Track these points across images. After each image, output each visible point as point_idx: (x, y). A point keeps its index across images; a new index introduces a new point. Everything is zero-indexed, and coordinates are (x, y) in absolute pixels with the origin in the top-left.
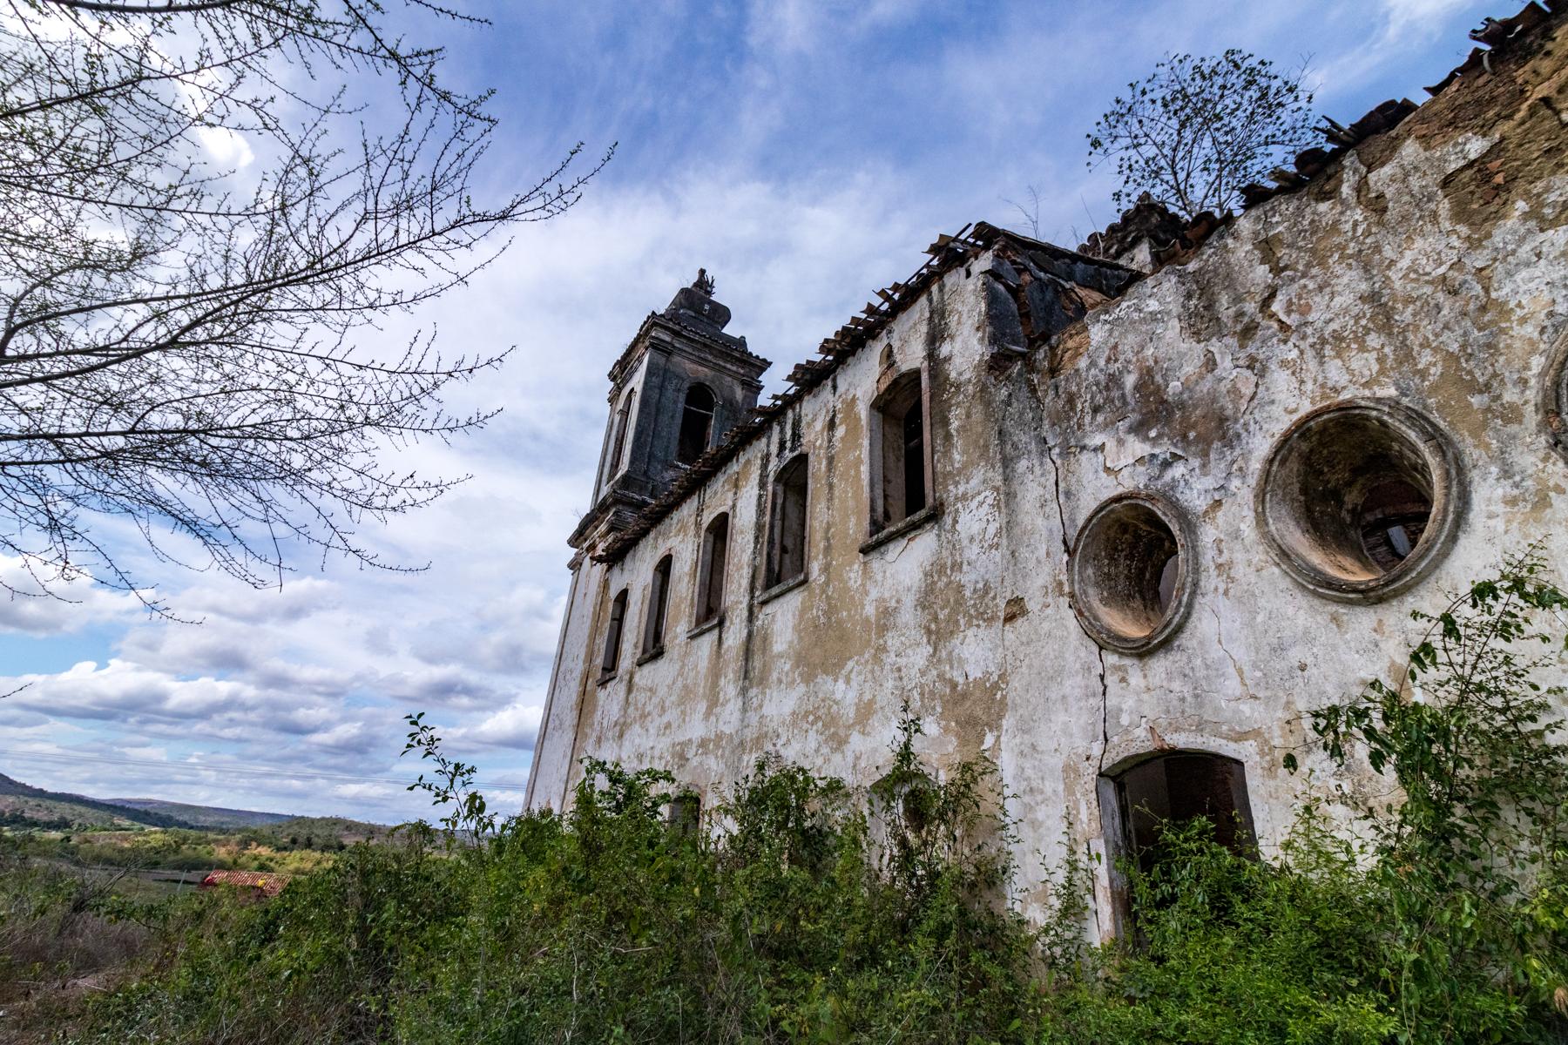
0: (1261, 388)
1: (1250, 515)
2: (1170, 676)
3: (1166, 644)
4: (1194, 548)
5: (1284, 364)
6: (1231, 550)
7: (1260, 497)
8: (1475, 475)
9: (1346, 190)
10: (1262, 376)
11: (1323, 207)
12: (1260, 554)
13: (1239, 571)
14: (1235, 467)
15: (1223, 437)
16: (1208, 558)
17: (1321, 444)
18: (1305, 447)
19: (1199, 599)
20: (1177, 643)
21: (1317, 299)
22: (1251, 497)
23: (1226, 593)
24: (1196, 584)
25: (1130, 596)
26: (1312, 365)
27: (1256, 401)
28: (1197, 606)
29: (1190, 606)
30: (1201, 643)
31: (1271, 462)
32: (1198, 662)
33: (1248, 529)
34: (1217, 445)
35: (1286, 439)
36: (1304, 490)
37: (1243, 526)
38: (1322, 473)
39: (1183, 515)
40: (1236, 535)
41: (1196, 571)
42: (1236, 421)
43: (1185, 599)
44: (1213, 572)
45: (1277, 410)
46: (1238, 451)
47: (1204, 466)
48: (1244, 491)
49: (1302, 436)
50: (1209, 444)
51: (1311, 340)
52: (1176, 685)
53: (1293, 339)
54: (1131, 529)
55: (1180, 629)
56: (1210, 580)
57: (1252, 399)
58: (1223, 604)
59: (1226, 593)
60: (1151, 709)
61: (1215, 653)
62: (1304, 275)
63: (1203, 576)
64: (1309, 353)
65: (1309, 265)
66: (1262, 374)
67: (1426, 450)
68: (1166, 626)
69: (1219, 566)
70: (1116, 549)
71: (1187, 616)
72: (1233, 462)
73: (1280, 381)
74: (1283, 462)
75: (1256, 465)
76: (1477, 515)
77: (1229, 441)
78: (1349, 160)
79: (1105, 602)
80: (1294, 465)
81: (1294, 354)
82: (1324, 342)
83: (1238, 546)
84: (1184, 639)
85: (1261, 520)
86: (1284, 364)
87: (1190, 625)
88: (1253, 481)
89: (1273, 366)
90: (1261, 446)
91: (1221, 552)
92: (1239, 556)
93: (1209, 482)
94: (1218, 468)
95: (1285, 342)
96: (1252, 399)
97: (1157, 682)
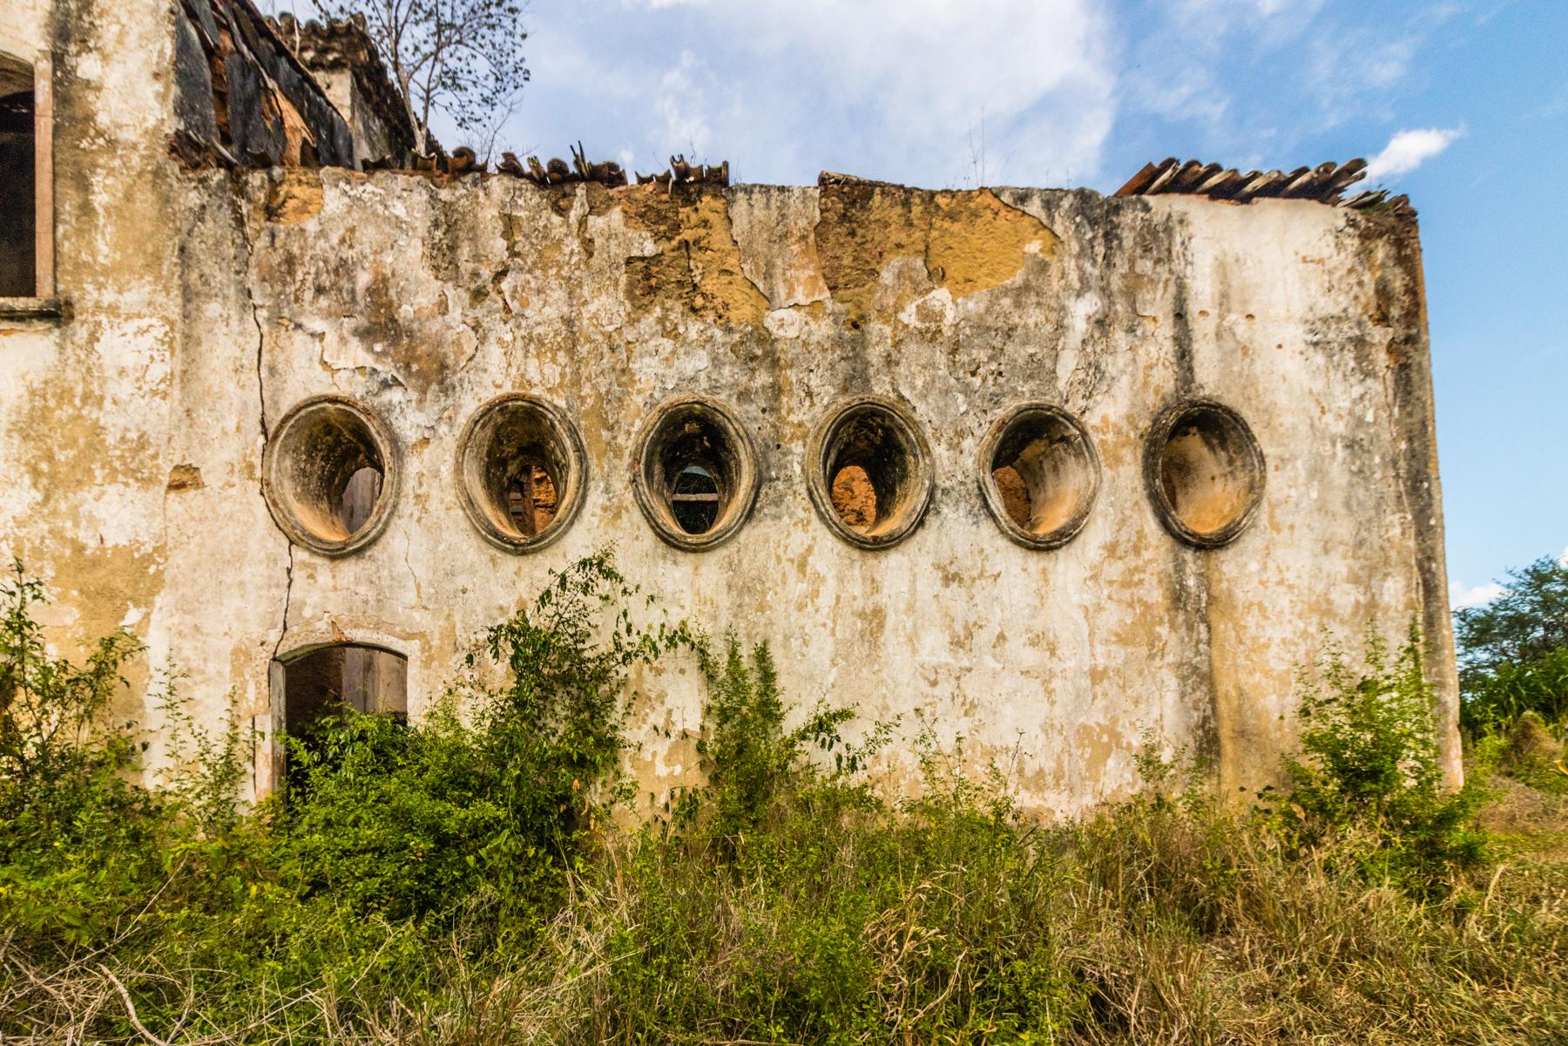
0: (479, 354)
1: (450, 461)
2: (357, 581)
3: (359, 552)
4: (399, 474)
5: (500, 341)
6: (430, 486)
7: (462, 448)
8: (592, 484)
9: (574, 215)
10: (482, 343)
11: (556, 219)
12: (450, 496)
13: (433, 505)
14: (446, 414)
15: (441, 382)
16: (410, 486)
17: (510, 422)
18: (500, 420)
19: (395, 520)
20: (368, 553)
21: (535, 299)
22: (454, 446)
23: (419, 520)
24: (395, 506)
25: (319, 497)
26: (519, 354)
27: (471, 364)
28: (392, 525)
29: (387, 523)
30: (391, 558)
31: (476, 422)
32: (385, 573)
33: (447, 471)
34: (434, 387)
35: (490, 409)
36: (489, 454)
37: (443, 469)
38: (501, 443)
39: (394, 440)
40: (436, 474)
41: (398, 495)
42: (454, 373)
43: (384, 517)
44: (412, 500)
45: (487, 379)
46: (450, 401)
47: (420, 401)
48: (449, 438)
49: (501, 410)
50: (429, 384)
51: (523, 332)
52: (362, 589)
53: (511, 324)
54: (335, 432)
55: (374, 541)
56: (408, 506)
57: (471, 359)
58: (414, 529)
59: (419, 520)
60: (336, 606)
61: (401, 568)
62: (530, 271)
63: (403, 501)
64: (519, 343)
65: (534, 263)
66: (483, 340)
67: (572, 456)
68: (363, 537)
69: (417, 496)
70: (315, 447)
71: (382, 532)
72: (445, 409)
73: (494, 353)
74: (483, 426)
75: (462, 420)
76: (586, 512)
77: (446, 390)
78: (581, 190)
79: (304, 496)
80: (489, 431)
81: (508, 337)
82: (531, 340)
83: (436, 484)
84: (375, 551)
85: (459, 469)
86: (500, 341)
87: (384, 540)
88: (457, 432)
89: (492, 339)
90: (470, 404)
91: (421, 484)
92: (435, 493)
93: (422, 419)
94: (432, 410)
95: (506, 323)
96: (471, 359)
97: (345, 583)
